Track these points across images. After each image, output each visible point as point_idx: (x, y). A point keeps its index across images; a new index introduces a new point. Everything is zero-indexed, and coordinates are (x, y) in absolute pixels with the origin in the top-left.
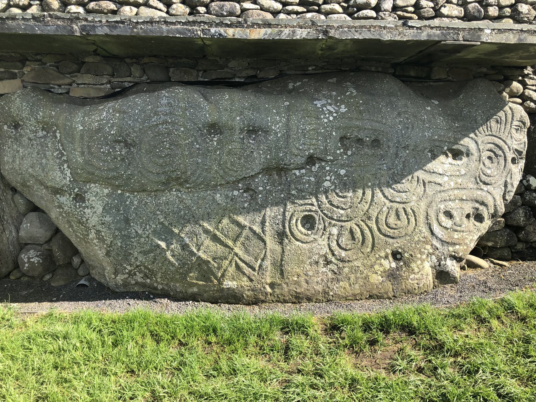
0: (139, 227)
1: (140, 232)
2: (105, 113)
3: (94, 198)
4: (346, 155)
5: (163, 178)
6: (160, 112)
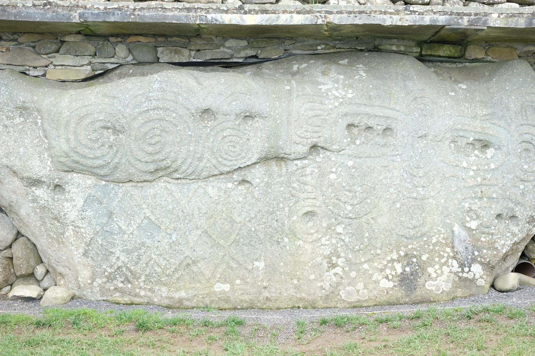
0: (123, 222)
1: (123, 228)
2: (93, 98)
3: (75, 190)
4: (354, 143)
5: (152, 167)
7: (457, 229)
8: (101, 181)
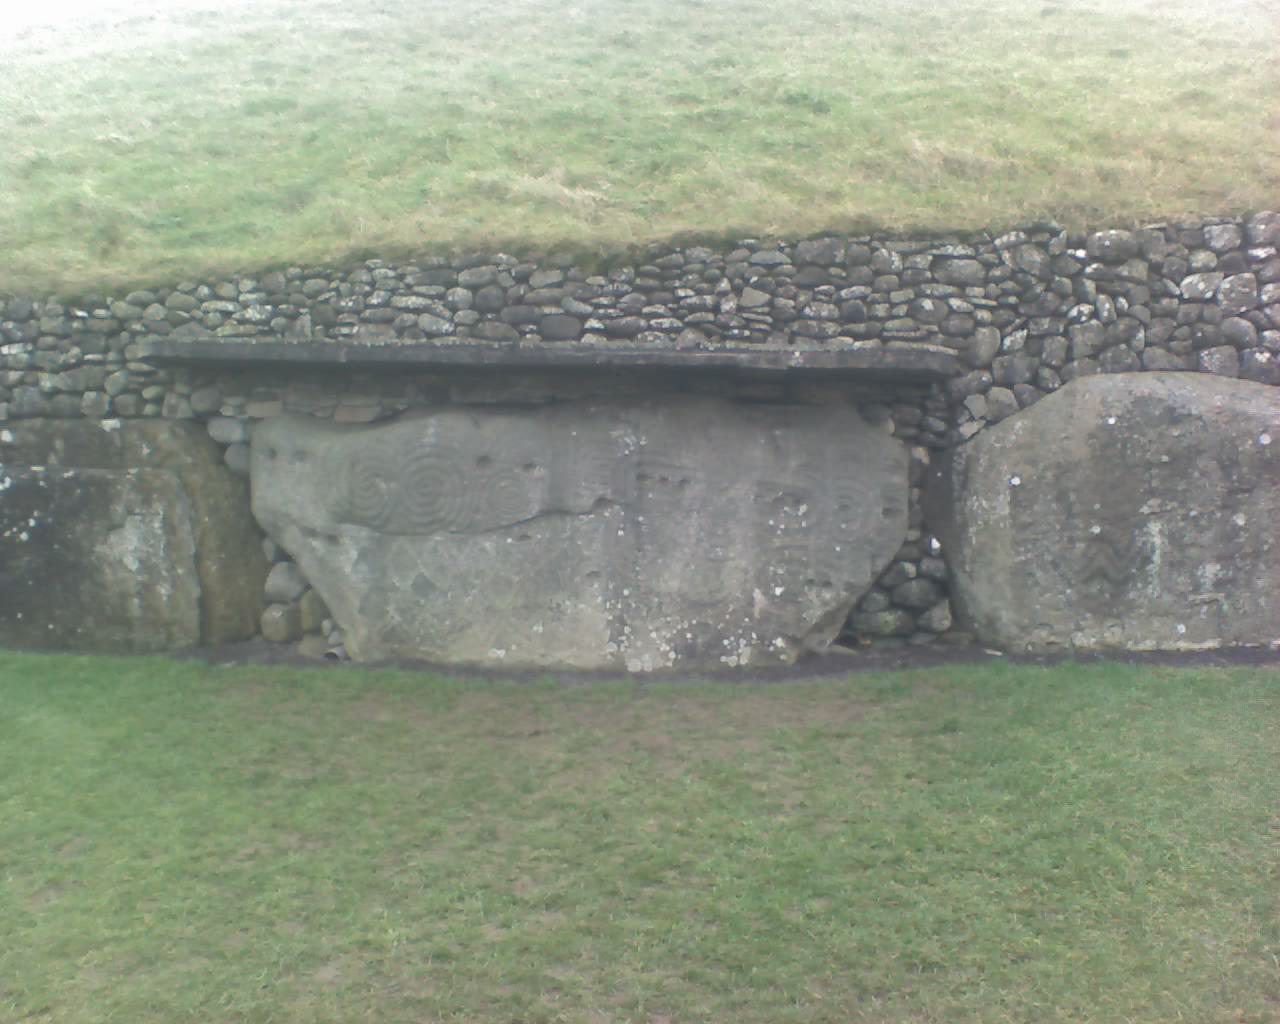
7: (758, 594)
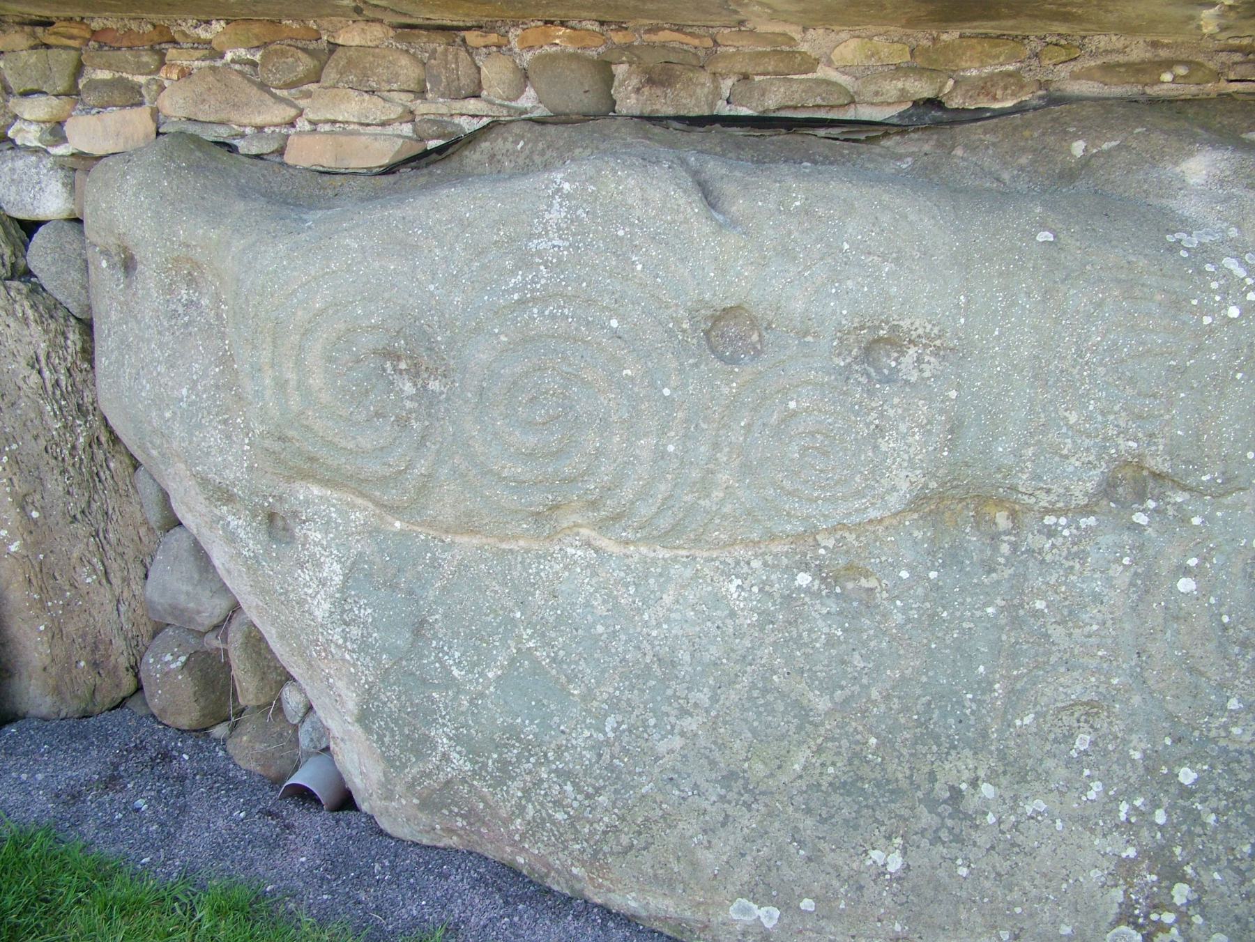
1: (456, 672)
5: (540, 499)
6: (539, 253)
8: (389, 518)
